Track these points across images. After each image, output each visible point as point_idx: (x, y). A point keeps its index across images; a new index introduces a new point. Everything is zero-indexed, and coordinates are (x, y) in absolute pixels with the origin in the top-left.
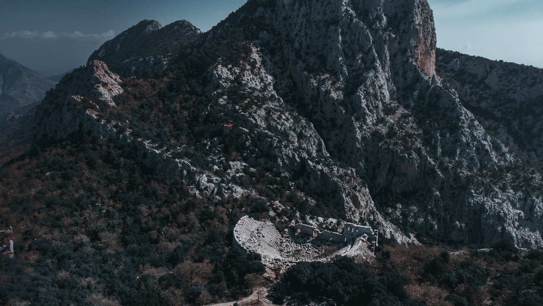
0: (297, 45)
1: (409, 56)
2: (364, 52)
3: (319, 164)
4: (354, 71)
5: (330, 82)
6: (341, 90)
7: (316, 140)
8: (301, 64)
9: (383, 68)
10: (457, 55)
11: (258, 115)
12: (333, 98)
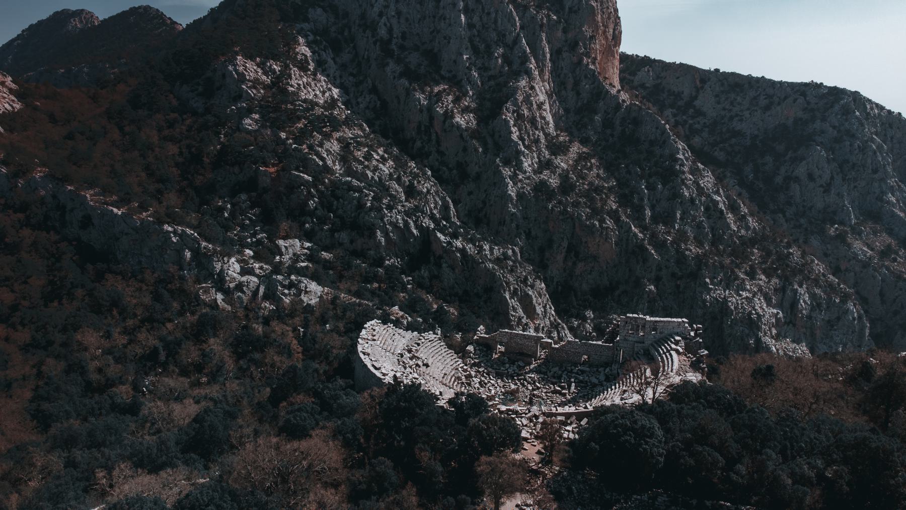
0: (383, 32)
1: (582, 54)
2: (506, 46)
3: (457, 238)
4: (490, 78)
5: (450, 98)
6: (471, 112)
7: (438, 199)
8: (392, 67)
9: (541, 73)
10: (646, 61)
11: (327, 150)
12: (459, 126)
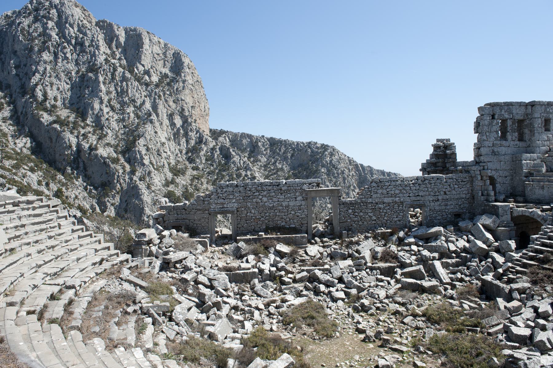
2: (135, 106)
6: (111, 147)
9: (161, 124)
10: (222, 132)
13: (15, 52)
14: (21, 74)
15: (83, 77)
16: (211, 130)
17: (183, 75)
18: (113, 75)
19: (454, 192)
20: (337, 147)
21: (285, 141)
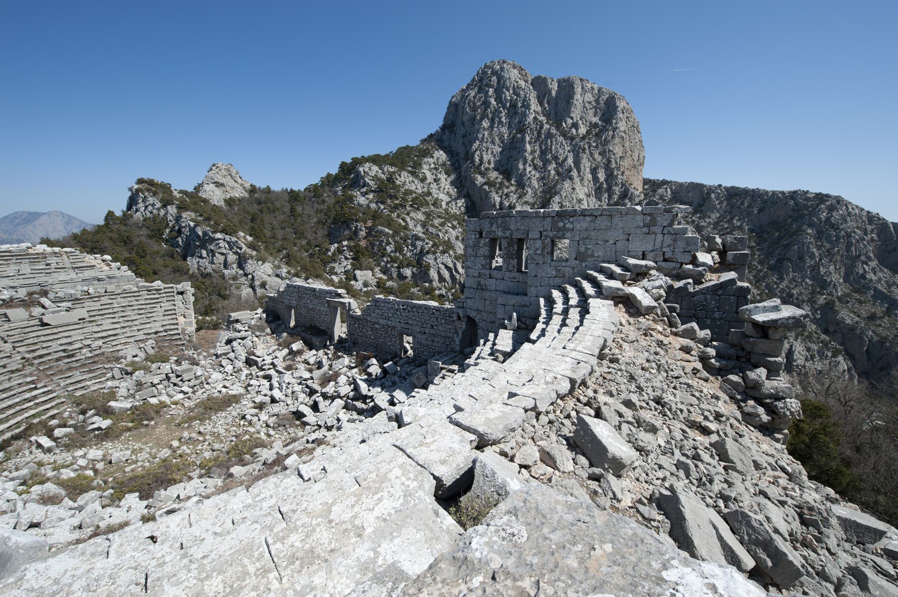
2: (556, 163)
9: (582, 180)
10: (664, 182)
13: (463, 124)
14: (467, 143)
15: (513, 139)
16: (646, 182)
17: (614, 121)
18: (539, 133)
19: (440, 328)
20: (847, 197)
21: (753, 190)
